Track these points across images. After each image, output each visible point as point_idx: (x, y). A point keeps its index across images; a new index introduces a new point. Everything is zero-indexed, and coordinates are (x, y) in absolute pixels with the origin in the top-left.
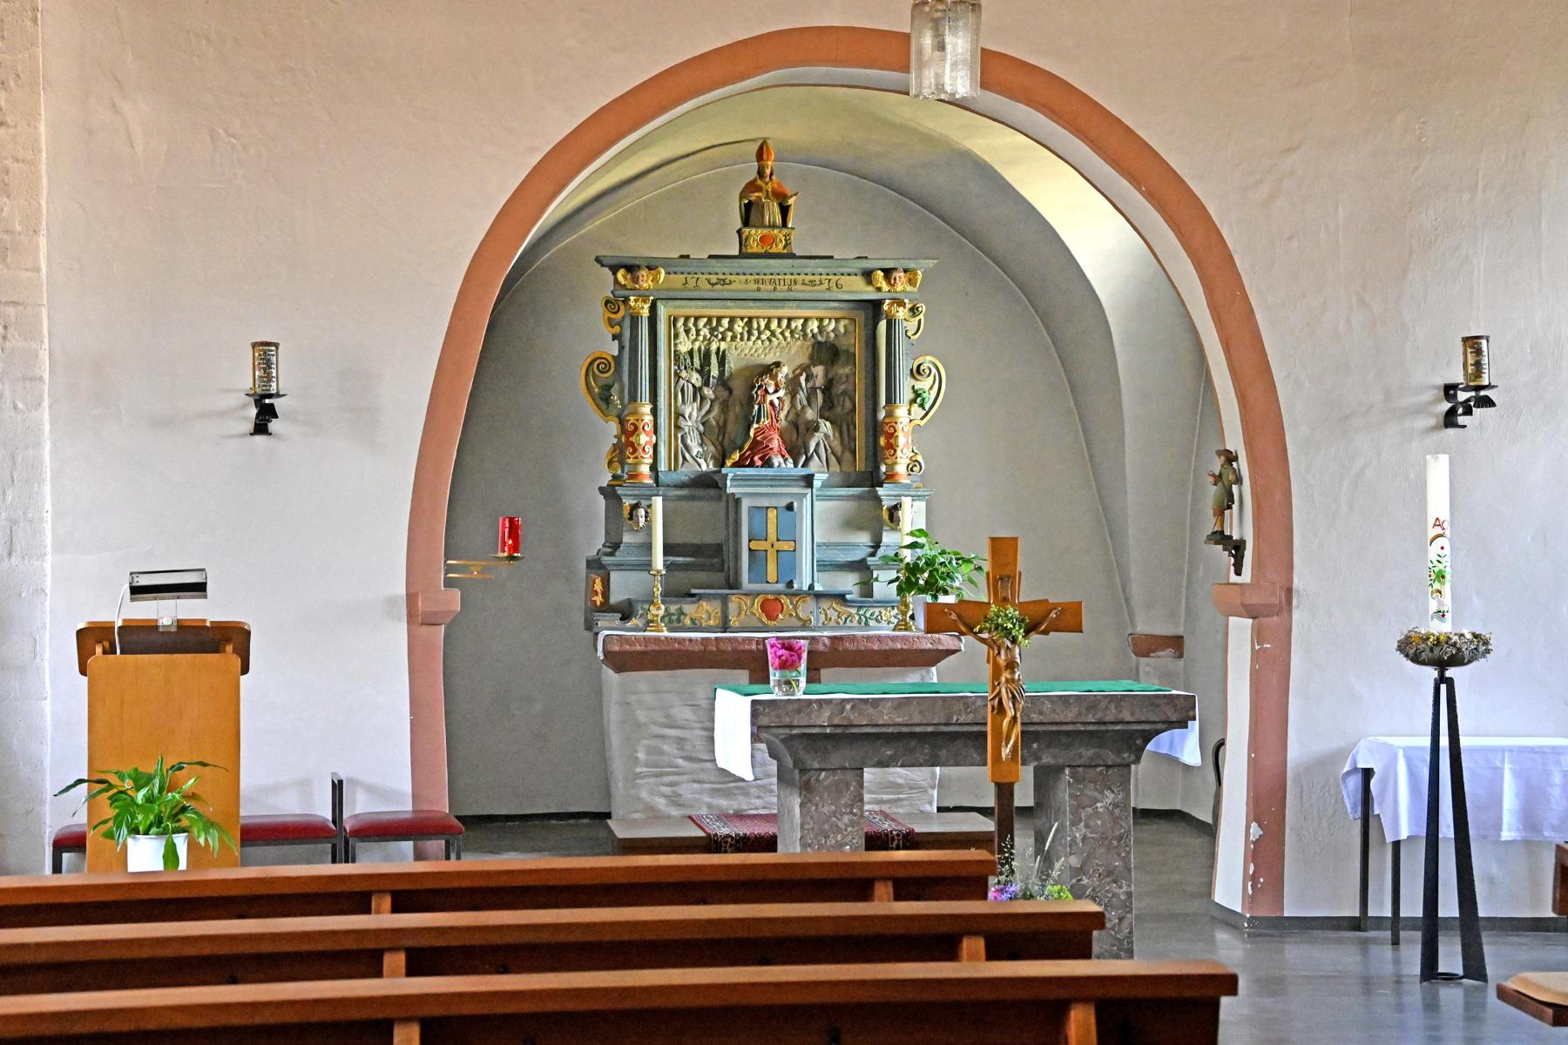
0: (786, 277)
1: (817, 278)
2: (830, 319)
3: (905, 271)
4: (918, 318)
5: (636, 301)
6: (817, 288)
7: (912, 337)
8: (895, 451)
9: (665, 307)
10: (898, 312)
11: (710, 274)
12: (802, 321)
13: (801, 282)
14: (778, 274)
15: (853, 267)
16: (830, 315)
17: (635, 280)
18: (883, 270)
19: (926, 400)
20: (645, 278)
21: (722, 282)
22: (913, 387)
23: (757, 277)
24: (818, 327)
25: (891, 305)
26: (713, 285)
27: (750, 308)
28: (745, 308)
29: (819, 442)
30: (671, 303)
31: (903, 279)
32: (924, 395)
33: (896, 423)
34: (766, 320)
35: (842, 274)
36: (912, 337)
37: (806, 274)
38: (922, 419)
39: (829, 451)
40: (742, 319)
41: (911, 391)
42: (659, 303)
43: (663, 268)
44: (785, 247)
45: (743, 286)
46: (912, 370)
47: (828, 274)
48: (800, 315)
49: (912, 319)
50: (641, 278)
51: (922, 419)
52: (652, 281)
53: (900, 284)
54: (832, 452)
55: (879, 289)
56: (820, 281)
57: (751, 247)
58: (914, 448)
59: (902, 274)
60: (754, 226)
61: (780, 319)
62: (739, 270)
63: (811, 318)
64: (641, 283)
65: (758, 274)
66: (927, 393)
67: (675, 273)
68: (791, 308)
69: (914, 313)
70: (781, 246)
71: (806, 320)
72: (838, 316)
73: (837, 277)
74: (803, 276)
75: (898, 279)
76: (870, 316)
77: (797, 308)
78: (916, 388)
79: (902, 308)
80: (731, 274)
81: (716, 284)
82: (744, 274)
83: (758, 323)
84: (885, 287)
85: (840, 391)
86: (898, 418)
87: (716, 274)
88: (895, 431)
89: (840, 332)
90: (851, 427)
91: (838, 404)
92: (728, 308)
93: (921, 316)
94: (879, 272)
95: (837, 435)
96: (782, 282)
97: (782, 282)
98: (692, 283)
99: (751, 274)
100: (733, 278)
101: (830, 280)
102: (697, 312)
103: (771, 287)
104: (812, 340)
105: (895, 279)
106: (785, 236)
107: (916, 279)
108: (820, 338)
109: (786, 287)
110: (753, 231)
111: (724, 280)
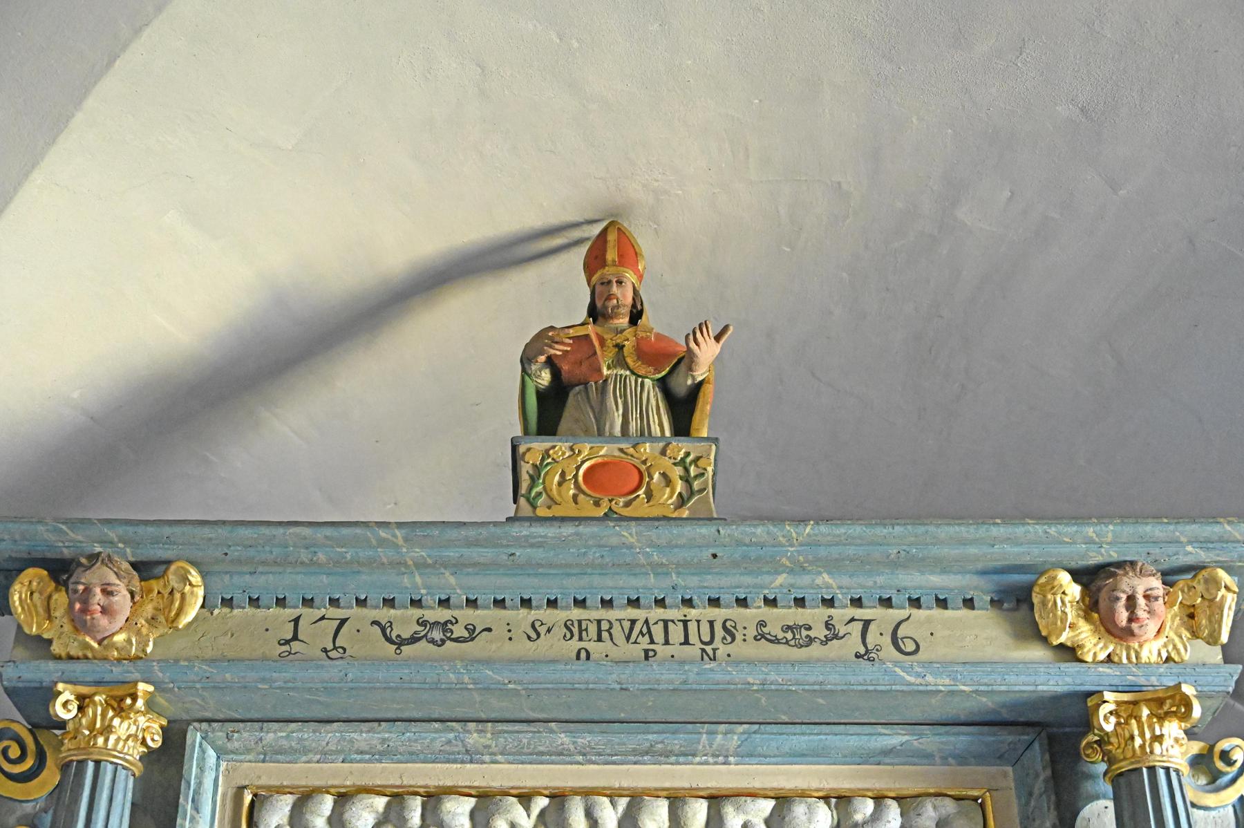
0: (693, 613)
1: (814, 615)
2: (879, 799)
3: (1169, 576)
5: (83, 702)
6: (815, 650)
9: (221, 753)
10: (1159, 739)
11: (389, 603)
12: (767, 806)
13: (751, 632)
14: (660, 603)
15: (942, 566)
16: (878, 785)
17: (80, 622)
18: (1076, 575)
20: (122, 600)
21: (437, 635)
23: (576, 613)
25: (1127, 712)
26: (400, 643)
27: (561, 755)
28: (539, 757)
30: (245, 735)
31: (1159, 605)
34: (623, 803)
35: (916, 603)
37: (771, 602)
40: (525, 798)
42: (195, 737)
43: (204, 575)
44: (682, 501)
45: (524, 648)
47: (857, 602)
48: (757, 784)
49: (1210, 800)
50: (98, 596)
52: (152, 621)
53: (1152, 627)
55: (1070, 653)
56: (828, 625)
57: (553, 501)
59: (1156, 583)
60: (572, 434)
61: (676, 800)
62: (512, 587)
63: (803, 795)
64: (103, 621)
65: (580, 603)
67: (254, 602)
68: (722, 756)
69: (1215, 776)
70: (667, 498)
71: (784, 800)
73: (896, 614)
74: (758, 611)
75: (1141, 602)
76: (1039, 786)
77: (747, 754)
79: (1173, 729)
80: (472, 603)
81: (414, 640)
82: (526, 603)
83: (589, 814)
84: (1093, 645)
87: (416, 603)
92: (471, 756)
94: (1064, 578)
96: (676, 633)
97: (676, 633)
98: (316, 636)
99: (552, 603)
100: (479, 617)
101: (867, 623)
102: (347, 774)
103: (636, 651)
105: (1131, 602)
107: (1216, 608)
109: (694, 651)
110: (561, 448)
111: (444, 626)
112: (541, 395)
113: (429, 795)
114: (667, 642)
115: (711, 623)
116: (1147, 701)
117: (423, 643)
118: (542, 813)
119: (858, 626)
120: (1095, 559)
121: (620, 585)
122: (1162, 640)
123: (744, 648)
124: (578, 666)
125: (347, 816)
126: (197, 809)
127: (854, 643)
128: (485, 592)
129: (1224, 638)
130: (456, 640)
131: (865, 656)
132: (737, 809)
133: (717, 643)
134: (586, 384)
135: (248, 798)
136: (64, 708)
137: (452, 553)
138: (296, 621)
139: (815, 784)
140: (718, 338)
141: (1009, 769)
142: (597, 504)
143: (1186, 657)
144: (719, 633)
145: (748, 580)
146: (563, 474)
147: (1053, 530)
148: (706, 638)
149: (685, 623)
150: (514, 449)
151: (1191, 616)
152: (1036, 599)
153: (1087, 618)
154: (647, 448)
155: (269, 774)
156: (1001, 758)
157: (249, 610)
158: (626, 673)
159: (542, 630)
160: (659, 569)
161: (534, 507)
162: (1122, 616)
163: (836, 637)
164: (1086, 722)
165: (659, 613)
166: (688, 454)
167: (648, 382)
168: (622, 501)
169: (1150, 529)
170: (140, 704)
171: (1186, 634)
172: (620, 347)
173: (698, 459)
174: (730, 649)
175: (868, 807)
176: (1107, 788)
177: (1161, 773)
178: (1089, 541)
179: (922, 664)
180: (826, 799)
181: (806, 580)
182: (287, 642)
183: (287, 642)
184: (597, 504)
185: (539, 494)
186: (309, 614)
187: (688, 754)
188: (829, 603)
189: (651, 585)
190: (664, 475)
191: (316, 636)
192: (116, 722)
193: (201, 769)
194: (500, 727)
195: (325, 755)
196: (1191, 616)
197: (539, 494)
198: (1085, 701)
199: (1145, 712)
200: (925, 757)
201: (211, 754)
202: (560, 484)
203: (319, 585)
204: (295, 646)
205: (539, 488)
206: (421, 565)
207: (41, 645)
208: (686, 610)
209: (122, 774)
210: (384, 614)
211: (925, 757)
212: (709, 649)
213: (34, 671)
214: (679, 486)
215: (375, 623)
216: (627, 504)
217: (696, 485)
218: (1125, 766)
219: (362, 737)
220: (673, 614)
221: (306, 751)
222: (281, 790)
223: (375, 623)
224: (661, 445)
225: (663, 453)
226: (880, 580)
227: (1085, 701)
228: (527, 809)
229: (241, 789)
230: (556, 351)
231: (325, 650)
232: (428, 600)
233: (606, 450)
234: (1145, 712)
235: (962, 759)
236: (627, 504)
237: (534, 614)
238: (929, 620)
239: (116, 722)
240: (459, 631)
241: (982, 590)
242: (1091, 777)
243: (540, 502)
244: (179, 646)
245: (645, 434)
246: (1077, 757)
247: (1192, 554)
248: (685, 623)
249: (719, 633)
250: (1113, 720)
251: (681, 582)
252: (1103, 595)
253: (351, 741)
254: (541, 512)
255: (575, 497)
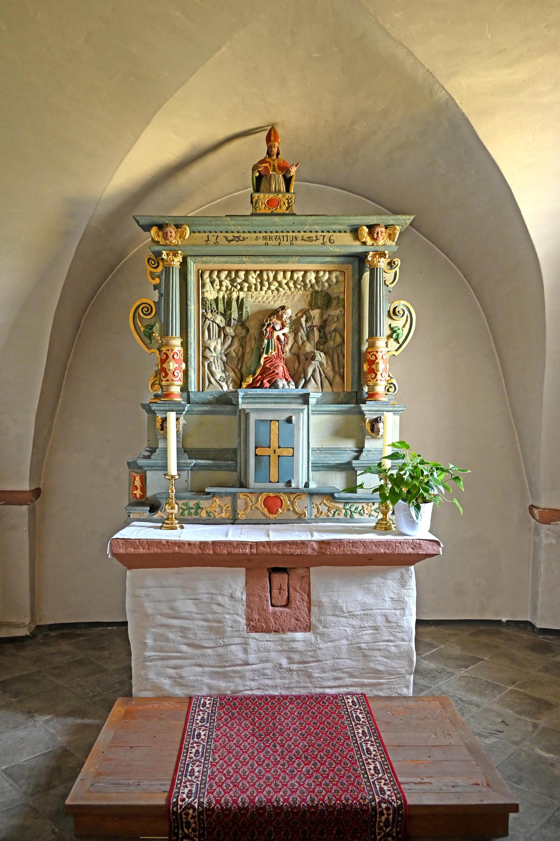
0: (289, 234)
1: (313, 235)
2: (325, 271)
3: (386, 227)
4: (394, 271)
6: (313, 243)
7: (390, 286)
8: (376, 375)
9: (194, 262)
11: (227, 232)
12: (302, 273)
13: (301, 238)
14: (282, 232)
15: (340, 224)
18: (368, 226)
19: (400, 336)
21: (237, 239)
22: (390, 325)
23: (265, 234)
24: (316, 278)
25: (374, 256)
26: (230, 241)
27: (262, 262)
28: (257, 263)
29: (315, 368)
30: (199, 259)
31: (384, 234)
32: (399, 332)
33: (377, 352)
34: (274, 272)
35: (334, 232)
36: (390, 286)
37: (305, 232)
38: (396, 350)
39: (323, 376)
40: (255, 271)
41: (389, 328)
42: (189, 259)
44: (287, 209)
45: (254, 242)
46: (389, 312)
48: (301, 268)
49: (390, 271)
51: (396, 350)
53: (381, 238)
54: (326, 377)
55: (364, 243)
56: (316, 237)
57: (260, 209)
58: (390, 374)
59: (383, 229)
60: (264, 192)
61: (285, 272)
62: (251, 229)
63: (310, 271)
65: (266, 232)
66: (401, 330)
67: (199, 232)
68: (294, 263)
69: (392, 266)
70: (284, 208)
71: (306, 272)
72: (331, 269)
73: (330, 234)
74: (302, 234)
75: (380, 233)
76: (356, 269)
77: (299, 262)
78: (392, 326)
79: (382, 259)
80: (244, 232)
81: (232, 240)
82: (255, 232)
83: (267, 275)
84: (369, 241)
85: (332, 329)
86: (378, 348)
87: (232, 232)
88: (376, 358)
89: (333, 282)
90: (341, 356)
91: (331, 339)
92: (244, 263)
93: (397, 269)
94: (365, 228)
95: (329, 363)
96: (285, 238)
97: (285, 238)
98: (212, 240)
99: (260, 232)
100: (245, 235)
101: (324, 236)
103: (277, 243)
104: (311, 290)
105: (378, 233)
106: (287, 199)
107: (395, 234)
108: (316, 288)
109: (289, 243)
110: (262, 195)
111: (238, 237)
112: (256, 178)
113: (236, 271)
114: (283, 241)
115: (292, 236)
116: (378, 254)
117: (234, 241)
118: (258, 274)
119: (322, 237)
120: (372, 223)
121: (274, 229)
122: (383, 240)
123: (299, 242)
124: (265, 247)
125: (220, 275)
126: (191, 275)
127: (321, 241)
128: (246, 229)
129: (396, 240)
130: (241, 240)
131: (323, 244)
132: (297, 274)
133: (294, 241)
134: (267, 176)
135: (200, 272)
136: (164, 256)
137: (240, 222)
138: (208, 236)
139: (312, 268)
140: (296, 166)
141: (351, 265)
142: (269, 209)
143: (388, 244)
144: (294, 239)
145: (300, 227)
146: (262, 202)
147: (363, 218)
148: (291, 240)
149: (287, 236)
150: (252, 195)
151: (390, 235)
152: (359, 232)
153: (369, 236)
154: (280, 196)
155: (204, 266)
156: (349, 263)
157: (198, 234)
158: (275, 248)
159: (258, 238)
160: (283, 226)
161: (256, 210)
162: (376, 236)
163: (318, 239)
164: (367, 256)
165: (282, 234)
166: (289, 197)
167: (280, 175)
168: (274, 209)
169: (383, 217)
170: (179, 255)
171: (388, 239)
172: (274, 166)
173: (291, 198)
174: (296, 242)
175: (322, 273)
176: (369, 270)
177: (379, 269)
178: (371, 220)
179: (335, 246)
180: (314, 271)
181: (312, 227)
182: (207, 241)
183: (207, 241)
184: (269, 209)
185: (257, 207)
186: (211, 235)
187: (287, 262)
188: (317, 232)
189: (280, 228)
190: (284, 202)
191: (212, 240)
192: (175, 259)
193: (191, 266)
194: (250, 257)
195: (215, 263)
196: (390, 235)
197: (257, 207)
198: (366, 254)
199: (377, 256)
200: (334, 263)
201: (192, 263)
202: (261, 204)
203: (212, 228)
204: (209, 242)
205: (257, 206)
206: (233, 225)
207: (158, 243)
208: (287, 233)
209: (177, 269)
210: (226, 235)
211: (334, 263)
212: (292, 242)
213: (157, 248)
214: (287, 205)
215: (224, 237)
216: (276, 210)
217: (290, 205)
218: (372, 267)
219: (222, 259)
220: (285, 234)
221: (211, 262)
222: (207, 270)
223: (224, 237)
224: (283, 195)
225: (283, 196)
226: (328, 227)
227: (366, 254)
228: (255, 274)
229: (199, 270)
230: (260, 169)
231: (215, 243)
232: (235, 232)
233: (271, 196)
234: (377, 256)
235: (342, 263)
236: (276, 210)
237: (257, 234)
238: (337, 236)
239: (175, 259)
240: (241, 238)
241: (348, 229)
242: (367, 267)
243: (258, 209)
244: (185, 242)
245: (279, 192)
246: (364, 263)
247: (392, 222)
248: (287, 236)
249: (294, 239)
250: (371, 258)
251: (286, 228)
252: (372, 231)
253: (220, 260)
254: (258, 212)
255: (265, 207)
